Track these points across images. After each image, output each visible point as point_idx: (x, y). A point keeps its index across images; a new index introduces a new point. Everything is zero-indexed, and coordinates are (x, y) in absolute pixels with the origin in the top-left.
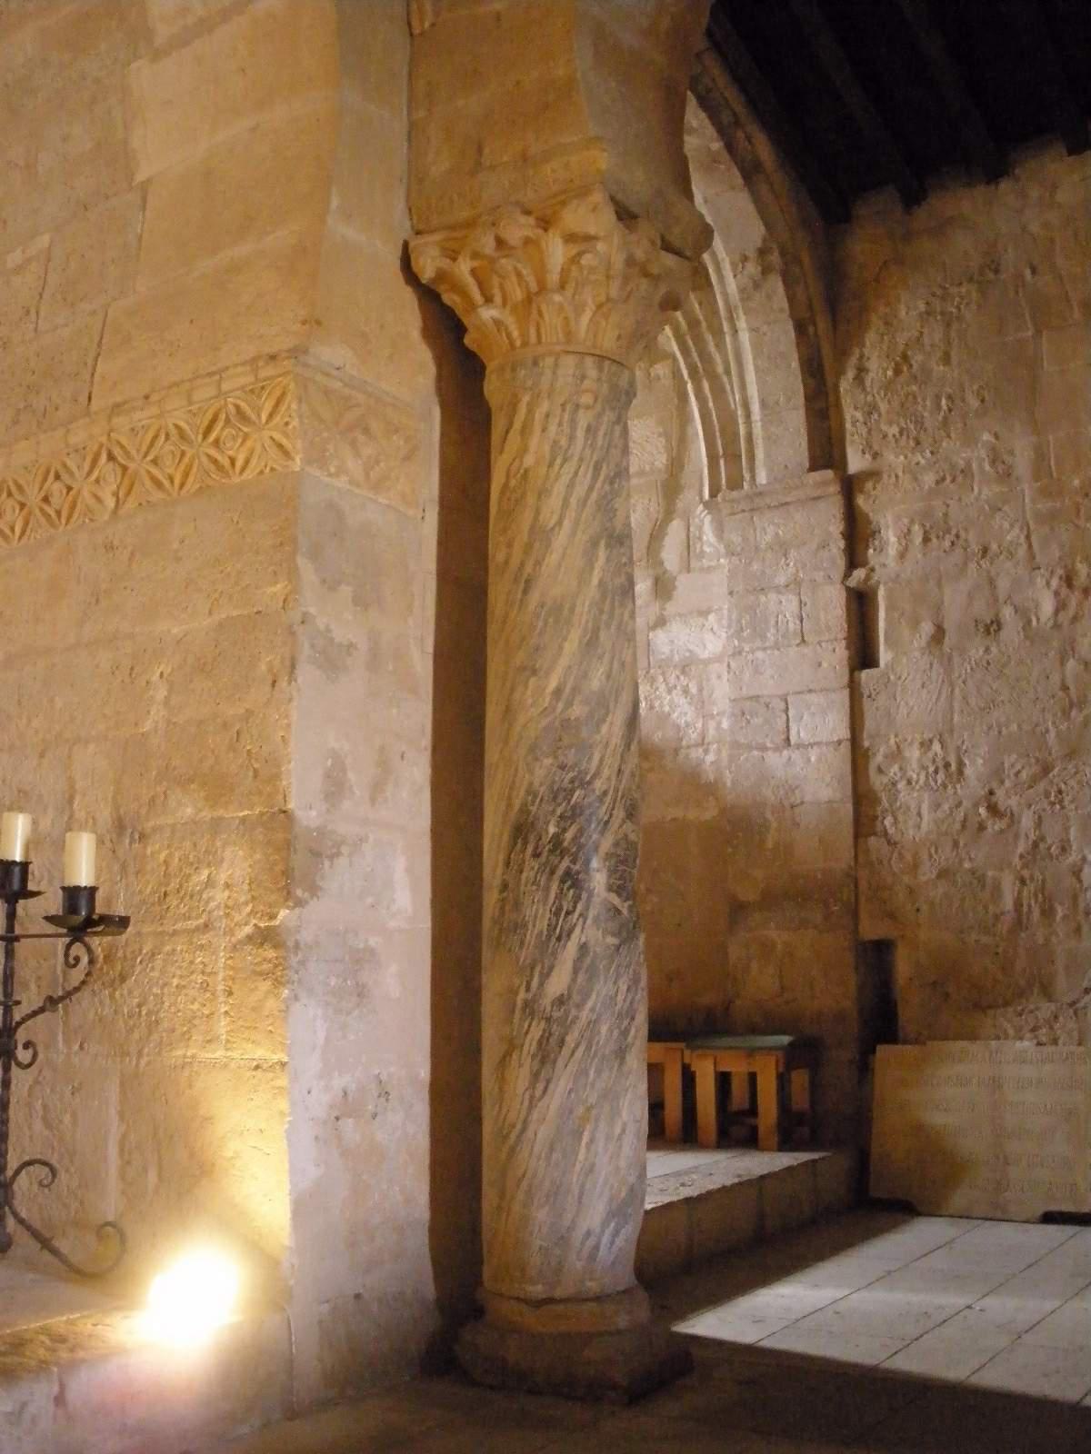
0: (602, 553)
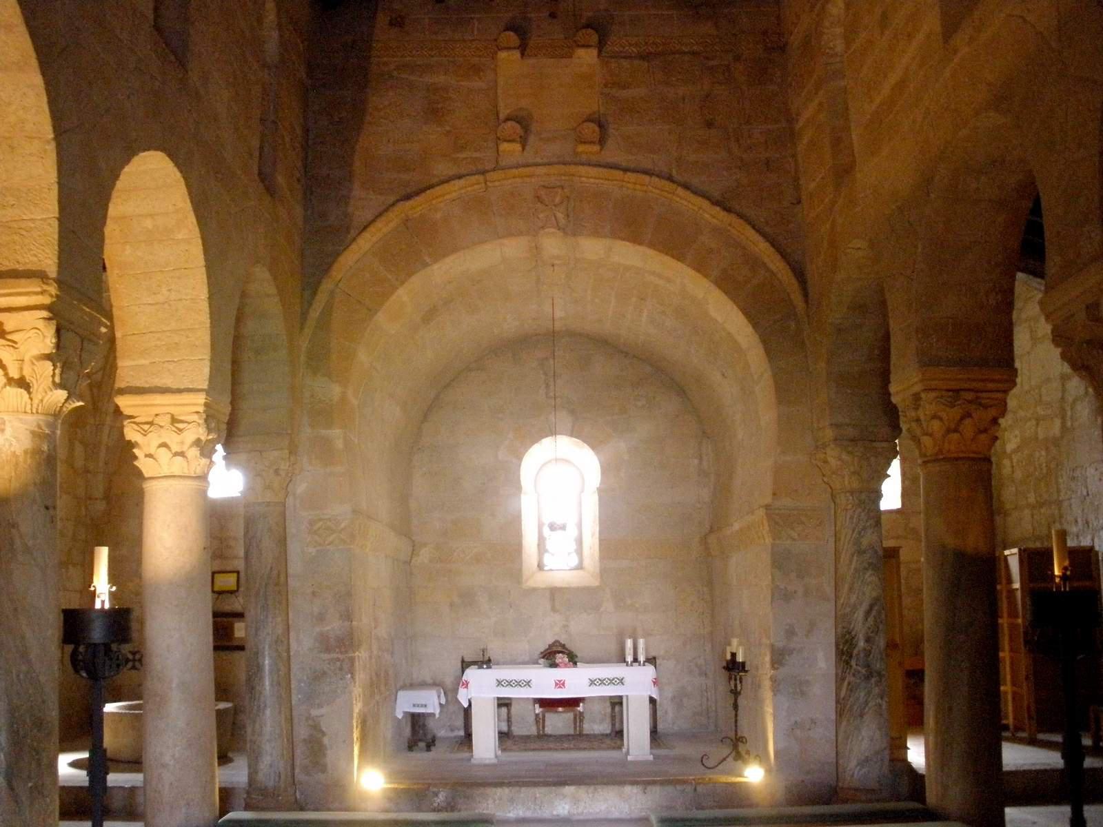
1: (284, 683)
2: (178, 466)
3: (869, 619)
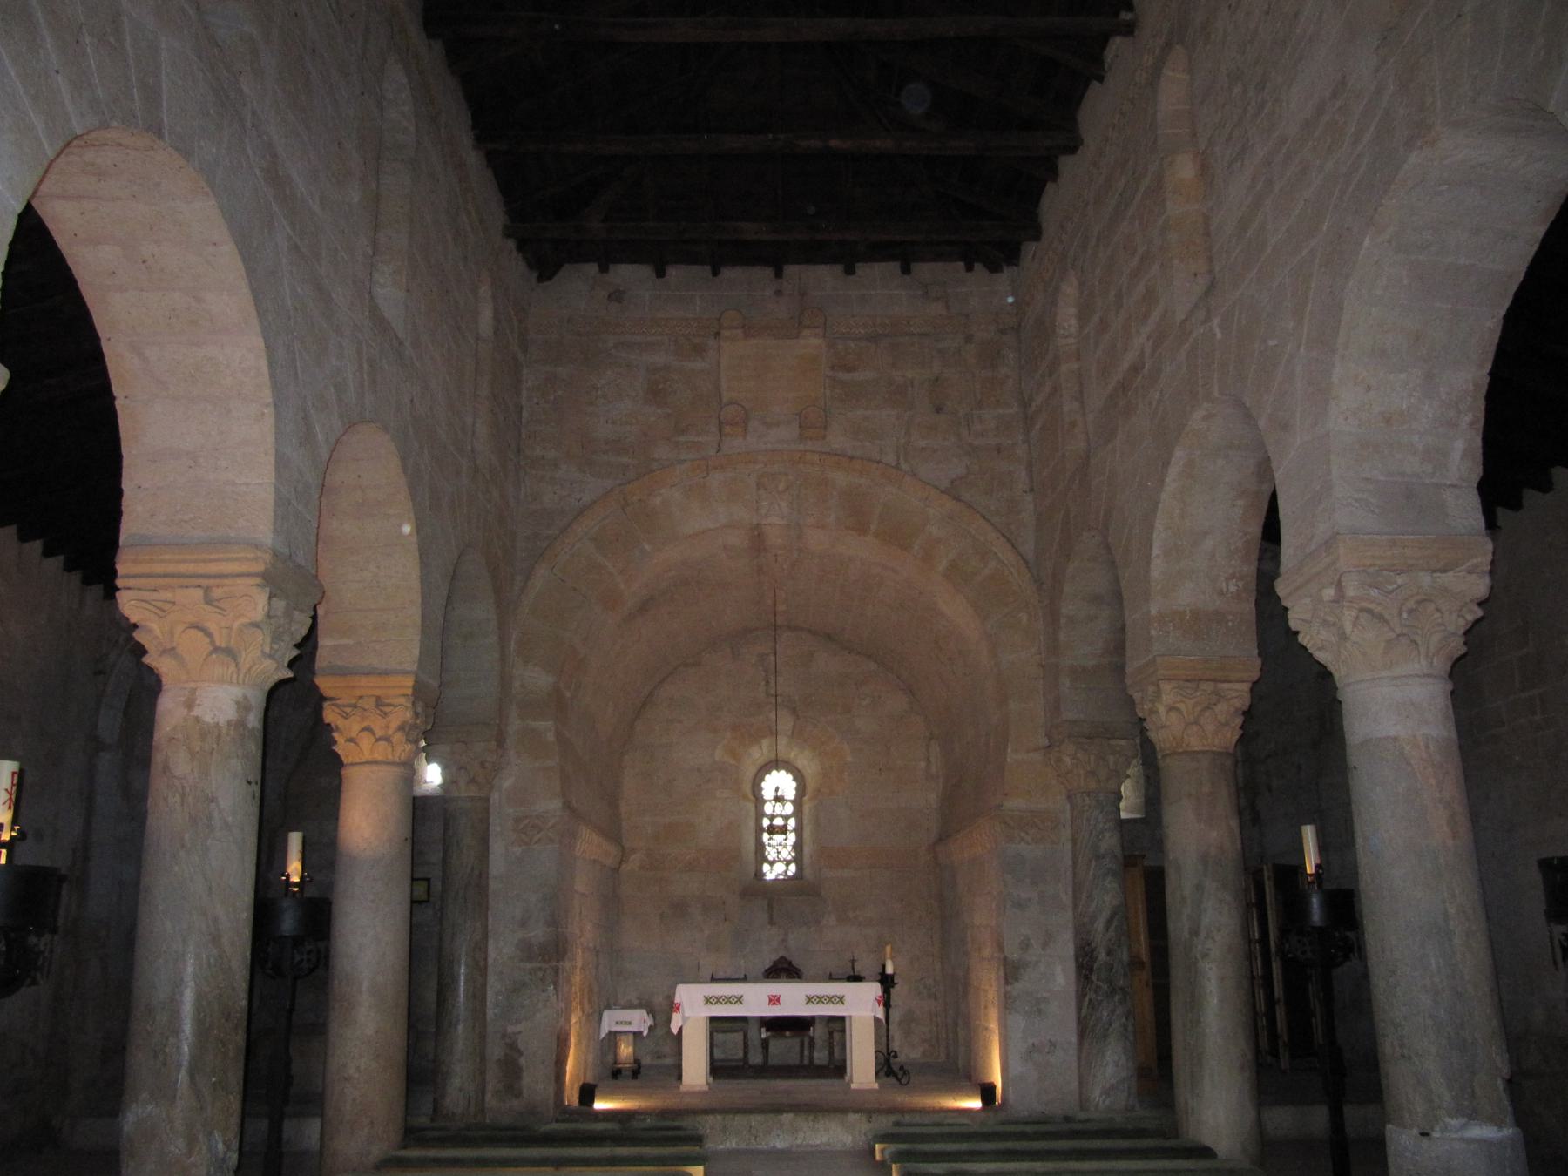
0: (1093, 863)
1: (478, 995)
2: (382, 748)
3: (1110, 930)
